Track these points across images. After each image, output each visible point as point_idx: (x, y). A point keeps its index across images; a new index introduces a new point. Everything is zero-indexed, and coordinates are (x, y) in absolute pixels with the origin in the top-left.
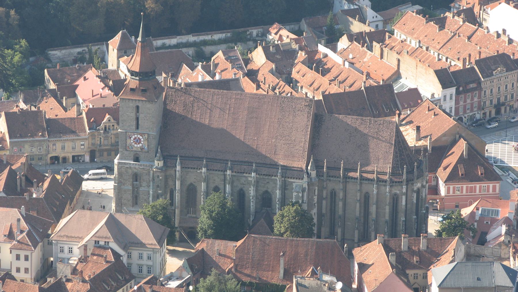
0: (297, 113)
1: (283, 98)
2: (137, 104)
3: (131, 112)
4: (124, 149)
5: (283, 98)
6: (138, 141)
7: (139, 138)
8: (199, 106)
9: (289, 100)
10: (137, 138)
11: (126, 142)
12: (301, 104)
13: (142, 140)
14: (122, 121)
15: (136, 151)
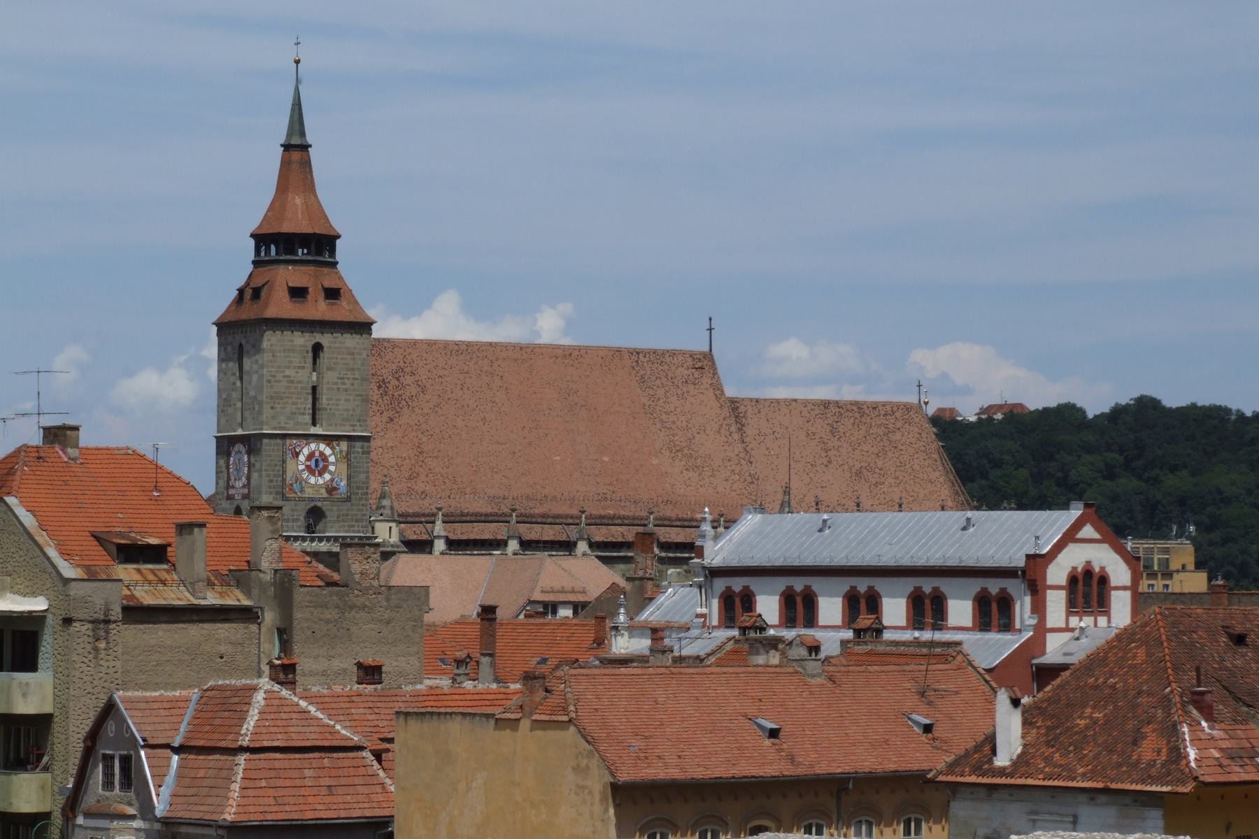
0: (685, 390)
1: (632, 354)
2: (318, 340)
3: (300, 368)
4: (277, 493)
5: (632, 354)
6: (318, 465)
7: (322, 454)
8: (420, 383)
9: (652, 359)
10: (317, 454)
11: (284, 472)
12: (685, 365)
13: (332, 459)
14: (272, 398)
15: (312, 499)
